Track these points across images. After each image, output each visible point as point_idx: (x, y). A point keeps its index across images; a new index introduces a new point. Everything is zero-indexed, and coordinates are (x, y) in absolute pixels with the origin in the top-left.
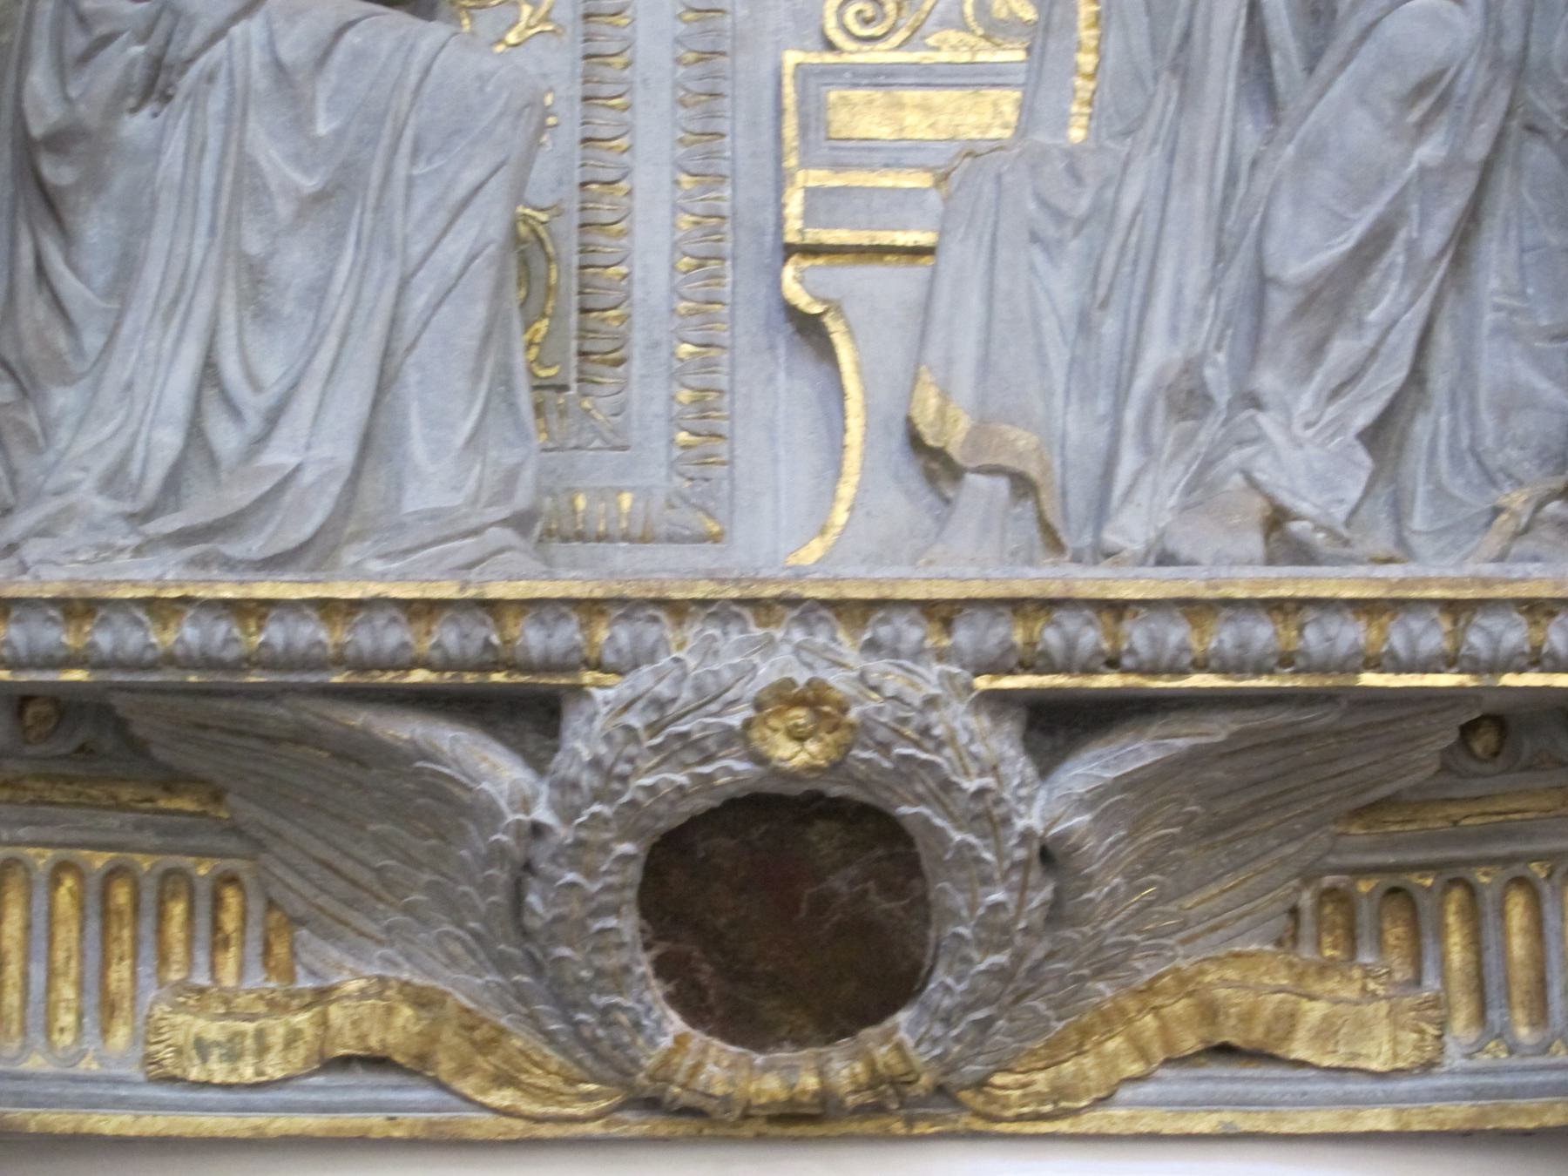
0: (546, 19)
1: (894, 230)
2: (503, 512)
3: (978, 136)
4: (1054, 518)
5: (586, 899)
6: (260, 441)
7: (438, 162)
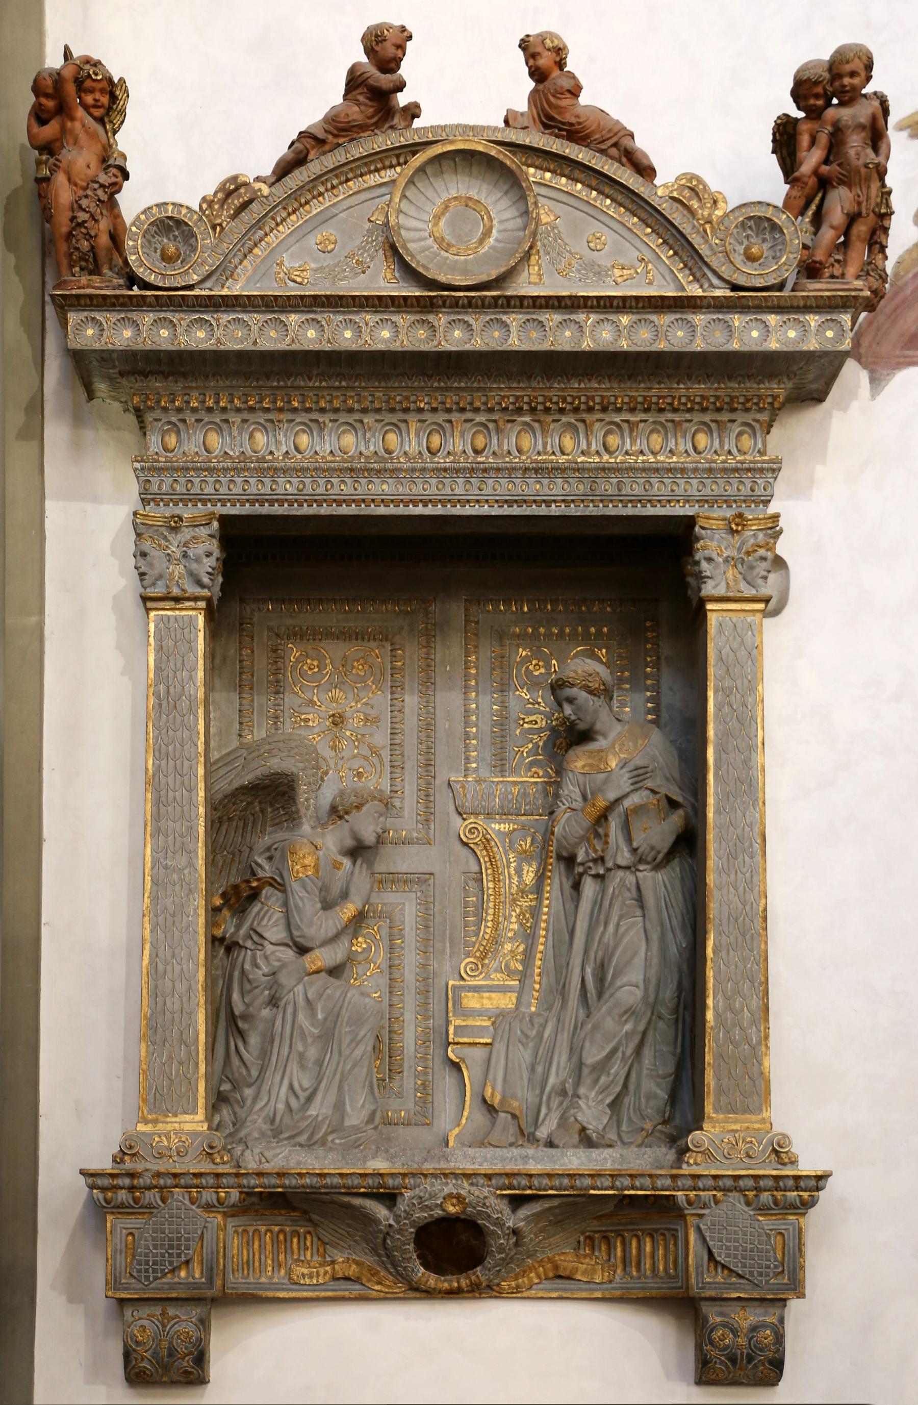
5: (401, 1241)
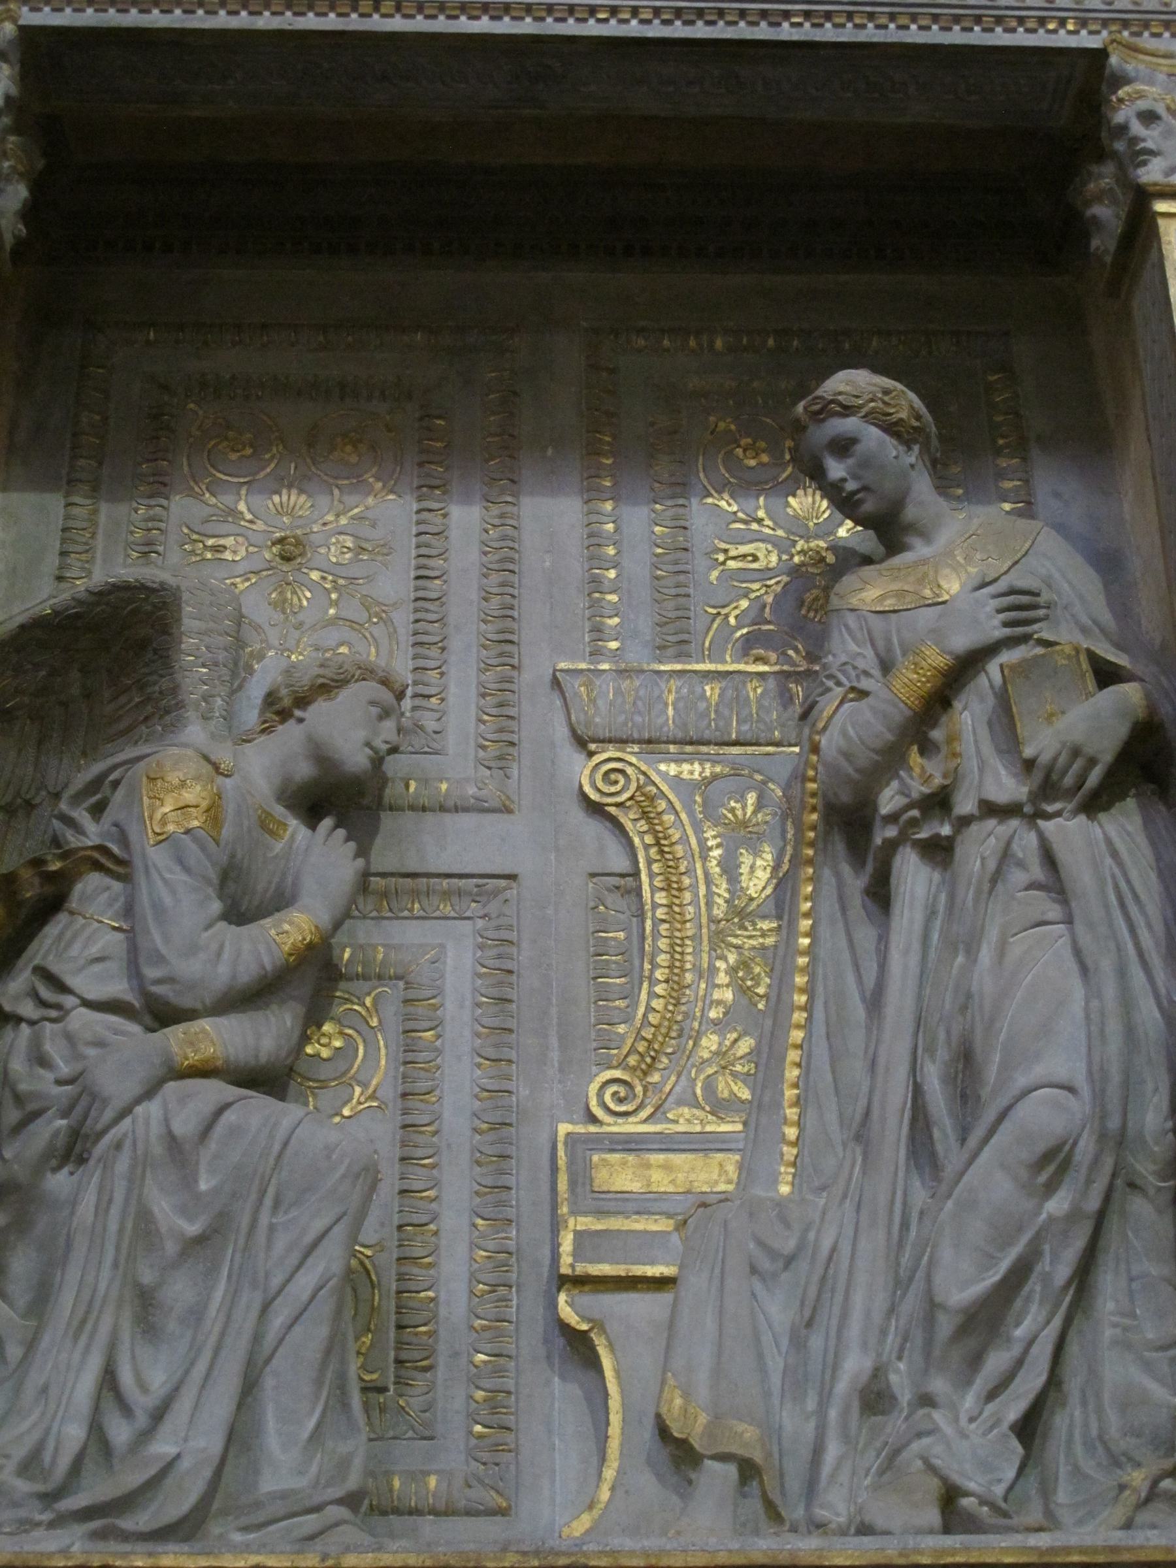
0: (373, 1097)
1: (644, 1264)
2: (338, 1492)
3: (708, 1190)
4: (775, 1496)
6: (146, 1435)
7: (294, 1213)
